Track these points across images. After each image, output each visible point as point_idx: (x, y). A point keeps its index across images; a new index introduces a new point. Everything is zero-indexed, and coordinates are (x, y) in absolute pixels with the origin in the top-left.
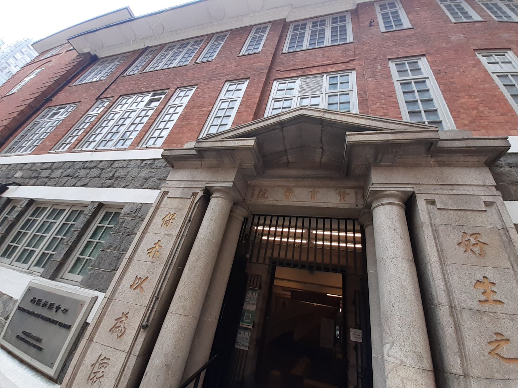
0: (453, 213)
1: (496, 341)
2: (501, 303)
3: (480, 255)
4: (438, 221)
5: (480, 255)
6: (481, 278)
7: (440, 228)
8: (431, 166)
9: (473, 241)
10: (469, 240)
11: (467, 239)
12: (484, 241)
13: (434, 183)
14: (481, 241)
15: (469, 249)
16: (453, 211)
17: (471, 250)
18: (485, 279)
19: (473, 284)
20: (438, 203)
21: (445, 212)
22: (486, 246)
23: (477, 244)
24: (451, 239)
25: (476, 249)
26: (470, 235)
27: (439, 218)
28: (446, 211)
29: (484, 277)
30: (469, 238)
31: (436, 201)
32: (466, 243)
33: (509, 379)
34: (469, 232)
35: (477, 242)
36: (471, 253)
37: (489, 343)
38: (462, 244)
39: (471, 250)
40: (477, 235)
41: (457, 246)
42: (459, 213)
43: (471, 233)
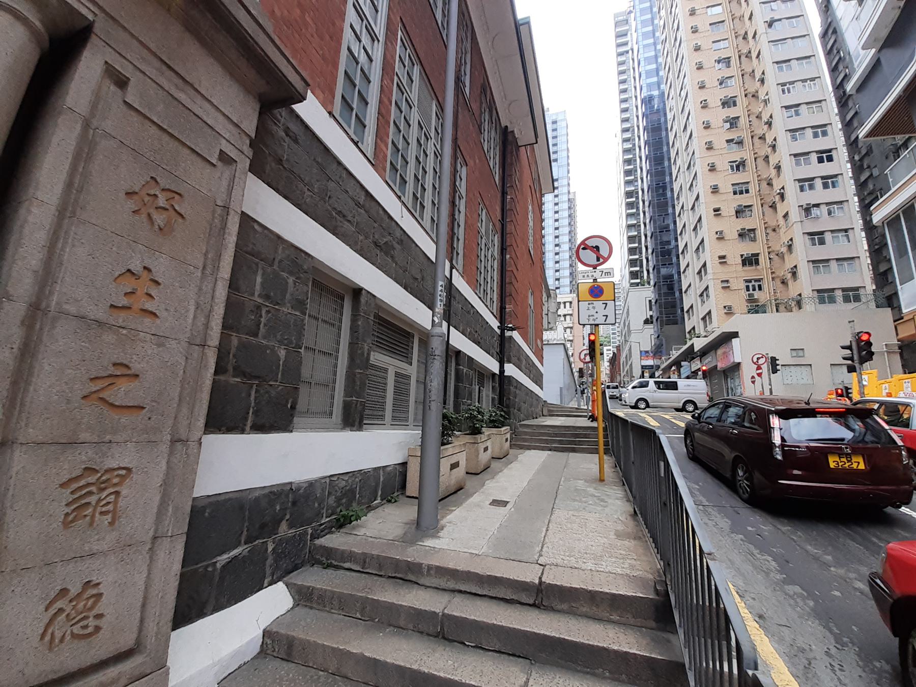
0: (153, 130)
1: (110, 376)
2: (152, 316)
3: (161, 229)
4: (108, 125)
5: (161, 229)
6: (136, 266)
7: (104, 145)
8: (169, 10)
9: (162, 202)
10: (155, 195)
11: (152, 192)
12: (182, 212)
13: (152, 46)
14: (177, 208)
15: (144, 211)
16: (154, 127)
17: (149, 215)
18: (146, 272)
19: (117, 274)
20: (131, 88)
21: (135, 118)
22: (180, 220)
23: (166, 209)
24: (113, 177)
25: (160, 219)
26: (163, 190)
27: (114, 121)
28: (141, 118)
29: (145, 268)
30: (157, 193)
31: (132, 83)
32: (147, 199)
33: (110, 441)
34: (163, 183)
35: (167, 207)
36: (145, 220)
37: (92, 379)
38: (136, 197)
39: (149, 215)
40: (177, 197)
41: (122, 195)
42: (166, 138)
43: (167, 187)
